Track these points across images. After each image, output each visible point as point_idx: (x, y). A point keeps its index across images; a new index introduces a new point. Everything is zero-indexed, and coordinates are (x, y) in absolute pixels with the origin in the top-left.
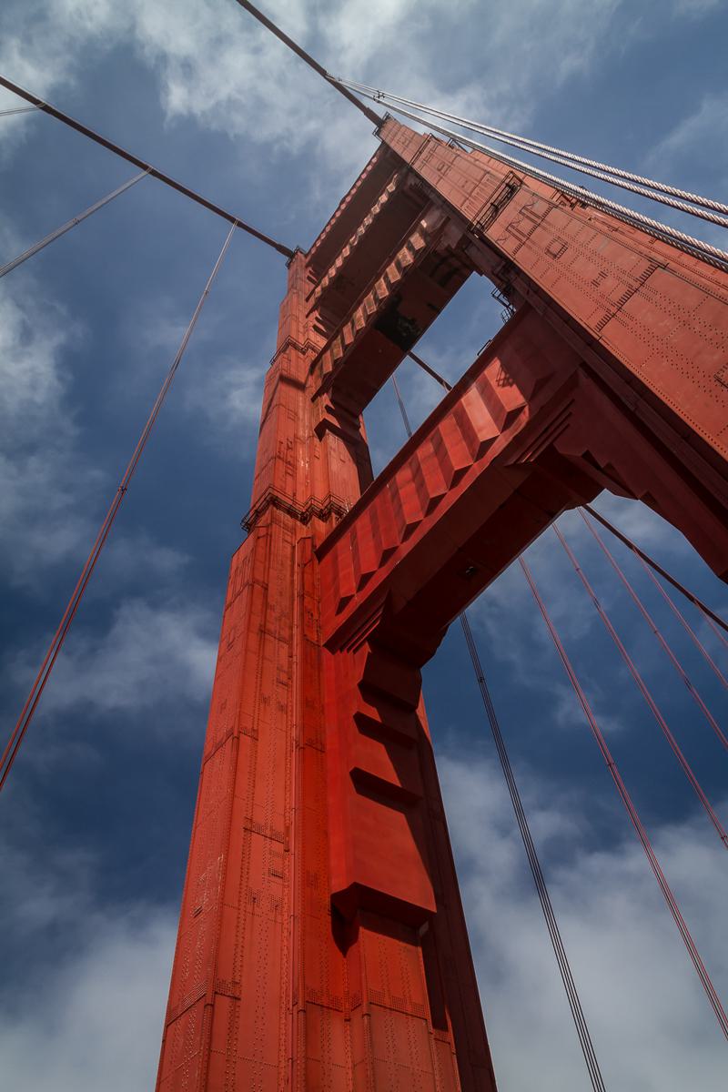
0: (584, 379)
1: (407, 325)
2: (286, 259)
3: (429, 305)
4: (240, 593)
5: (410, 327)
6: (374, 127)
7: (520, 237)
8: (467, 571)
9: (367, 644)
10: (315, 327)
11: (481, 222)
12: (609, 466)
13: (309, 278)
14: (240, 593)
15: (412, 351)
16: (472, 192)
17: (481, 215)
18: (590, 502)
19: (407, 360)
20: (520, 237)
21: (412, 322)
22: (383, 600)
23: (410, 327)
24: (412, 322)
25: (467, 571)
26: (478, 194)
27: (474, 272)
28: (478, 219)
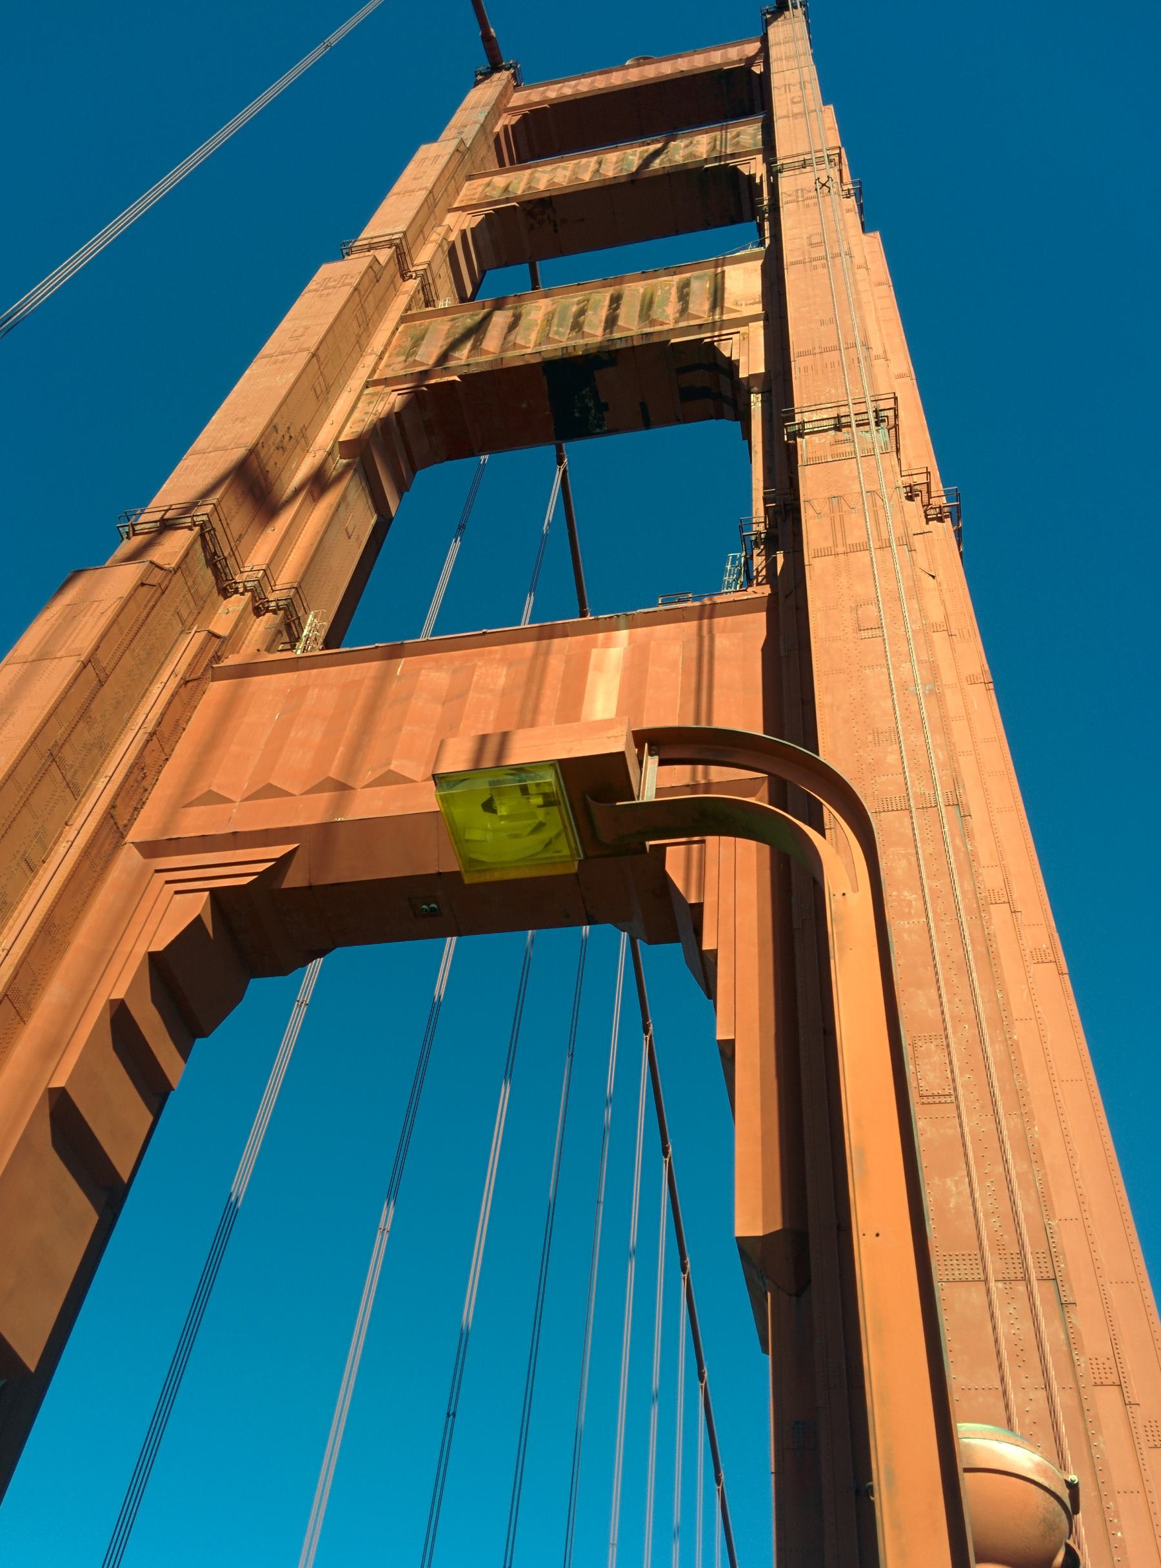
1: (591, 404)
3: (643, 405)
5: (593, 412)
7: (837, 520)
8: (424, 907)
11: (807, 426)
12: (714, 953)
13: (497, 140)
18: (651, 941)
20: (837, 520)
21: (603, 407)
22: (279, 851)
23: (593, 412)
24: (603, 407)
25: (424, 907)
27: (739, 422)
28: (806, 418)
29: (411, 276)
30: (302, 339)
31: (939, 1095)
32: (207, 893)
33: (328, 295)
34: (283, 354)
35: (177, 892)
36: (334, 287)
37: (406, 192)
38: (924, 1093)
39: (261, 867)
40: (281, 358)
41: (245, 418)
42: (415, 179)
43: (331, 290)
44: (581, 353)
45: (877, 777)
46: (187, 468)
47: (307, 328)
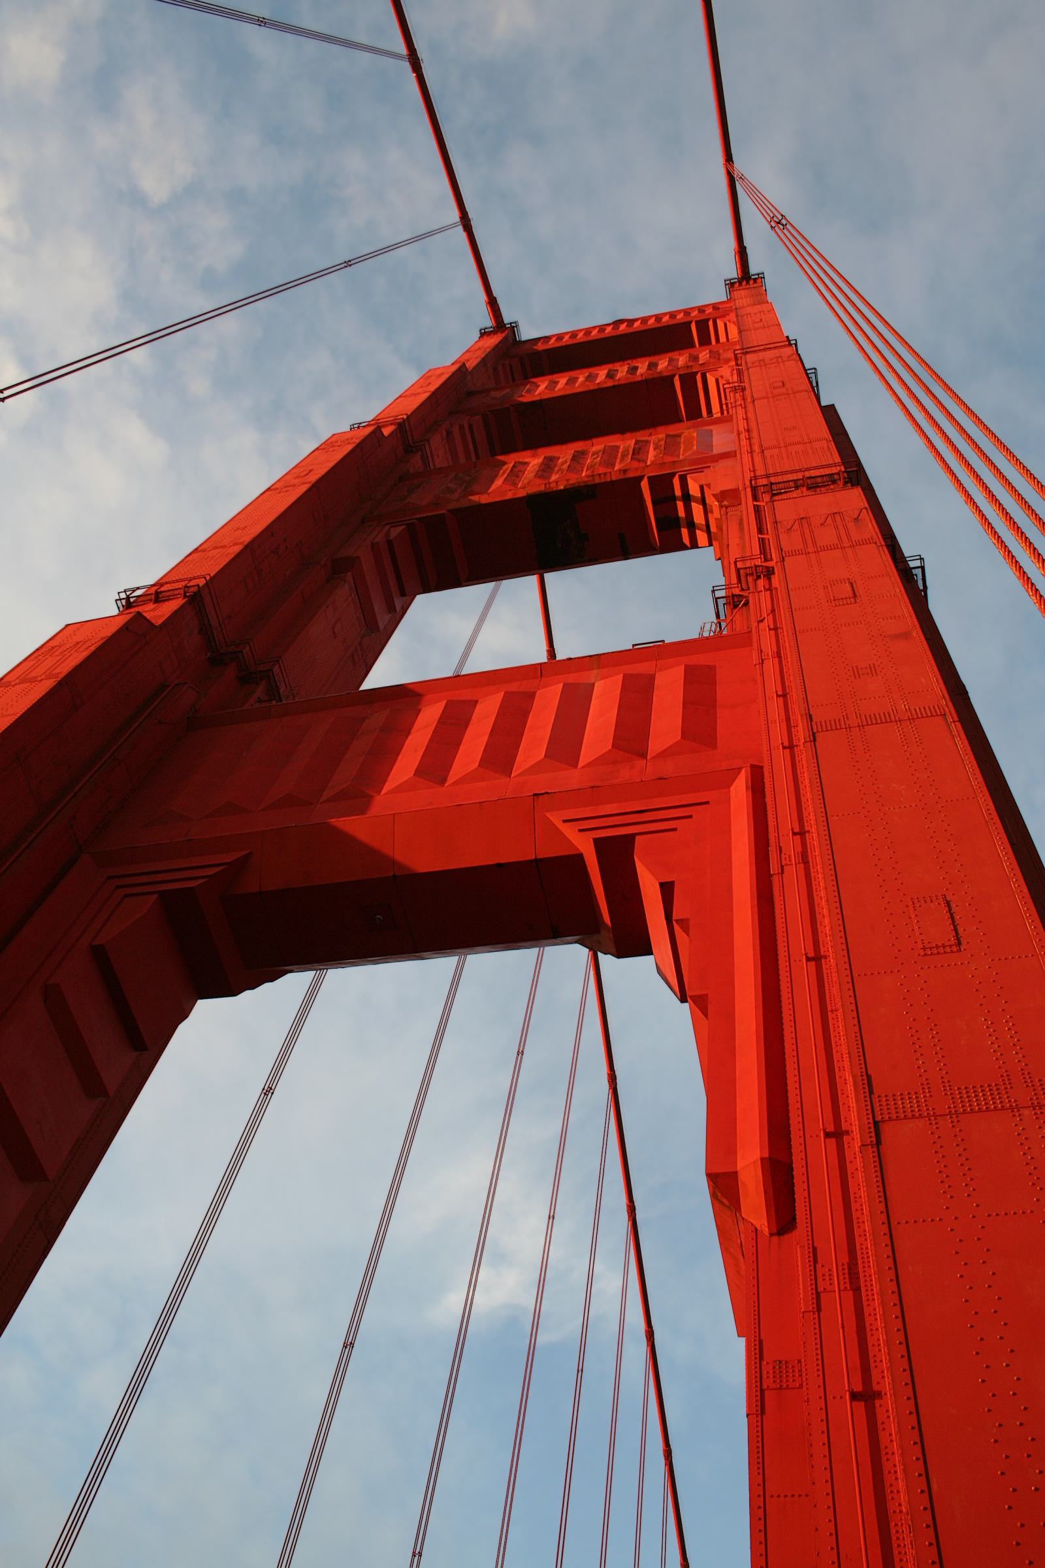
0: (740, 789)
2: (488, 322)
4: (34, 680)
6: (733, 272)
9: (155, 897)
10: (449, 433)
14: (34, 680)
15: (545, 575)
16: (790, 444)
17: (780, 479)
18: (619, 955)
19: (533, 580)
26: (797, 452)
29: (412, 451)
30: (306, 477)
31: (944, 946)
32: (155, 897)
33: (334, 450)
34: (286, 487)
35: (126, 896)
36: (339, 446)
37: (413, 394)
38: (927, 946)
39: (211, 872)
40: (286, 489)
41: (246, 527)
42: (421, 387)
43: (336, 448)
44: (562, 488)
45: (858, 702)
46: (188, 561)
47: (311, 471)
